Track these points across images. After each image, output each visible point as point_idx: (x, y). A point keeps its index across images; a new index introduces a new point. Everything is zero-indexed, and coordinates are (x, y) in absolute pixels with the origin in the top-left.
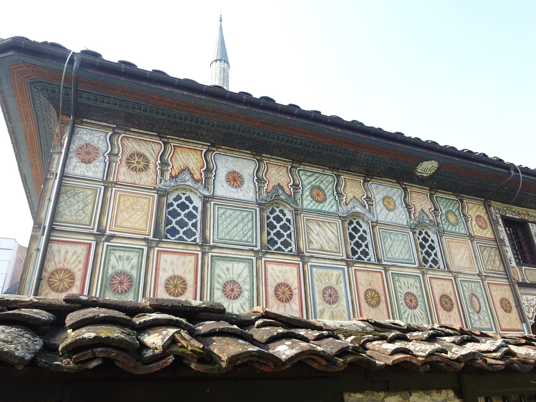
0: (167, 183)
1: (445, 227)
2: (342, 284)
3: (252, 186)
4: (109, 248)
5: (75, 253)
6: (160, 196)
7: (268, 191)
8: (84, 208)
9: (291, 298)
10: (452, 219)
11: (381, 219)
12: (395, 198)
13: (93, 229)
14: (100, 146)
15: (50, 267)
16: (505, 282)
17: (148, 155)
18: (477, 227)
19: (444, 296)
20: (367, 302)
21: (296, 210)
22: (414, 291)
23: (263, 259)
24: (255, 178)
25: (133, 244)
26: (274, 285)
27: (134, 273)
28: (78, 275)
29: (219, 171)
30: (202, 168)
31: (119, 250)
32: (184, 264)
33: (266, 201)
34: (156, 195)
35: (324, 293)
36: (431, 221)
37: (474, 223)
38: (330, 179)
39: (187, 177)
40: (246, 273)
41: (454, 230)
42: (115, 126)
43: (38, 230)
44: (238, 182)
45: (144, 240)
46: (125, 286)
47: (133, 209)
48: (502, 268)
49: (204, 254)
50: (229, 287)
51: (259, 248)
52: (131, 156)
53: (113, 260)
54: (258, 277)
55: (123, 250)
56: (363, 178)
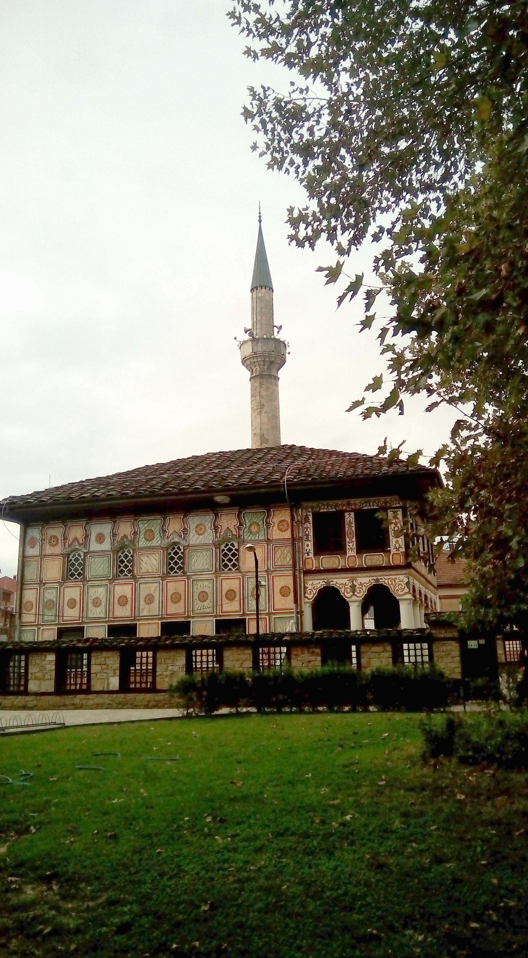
1: (246, 537)
3: (109, 540)
10: (254, 529)
11: (192, 543)
12: (206, 524)
15: (24, 601)
17: (58, 536)
18: (278, 531)
27: (55, 599)
35: (146, 598)
36: (233, 535)
37: (275, 528)
38: (159, 521)
39: (76, 543)
40: (104, 592)
45: (58, 582)
48: (291, 563)
54: (110, 593)
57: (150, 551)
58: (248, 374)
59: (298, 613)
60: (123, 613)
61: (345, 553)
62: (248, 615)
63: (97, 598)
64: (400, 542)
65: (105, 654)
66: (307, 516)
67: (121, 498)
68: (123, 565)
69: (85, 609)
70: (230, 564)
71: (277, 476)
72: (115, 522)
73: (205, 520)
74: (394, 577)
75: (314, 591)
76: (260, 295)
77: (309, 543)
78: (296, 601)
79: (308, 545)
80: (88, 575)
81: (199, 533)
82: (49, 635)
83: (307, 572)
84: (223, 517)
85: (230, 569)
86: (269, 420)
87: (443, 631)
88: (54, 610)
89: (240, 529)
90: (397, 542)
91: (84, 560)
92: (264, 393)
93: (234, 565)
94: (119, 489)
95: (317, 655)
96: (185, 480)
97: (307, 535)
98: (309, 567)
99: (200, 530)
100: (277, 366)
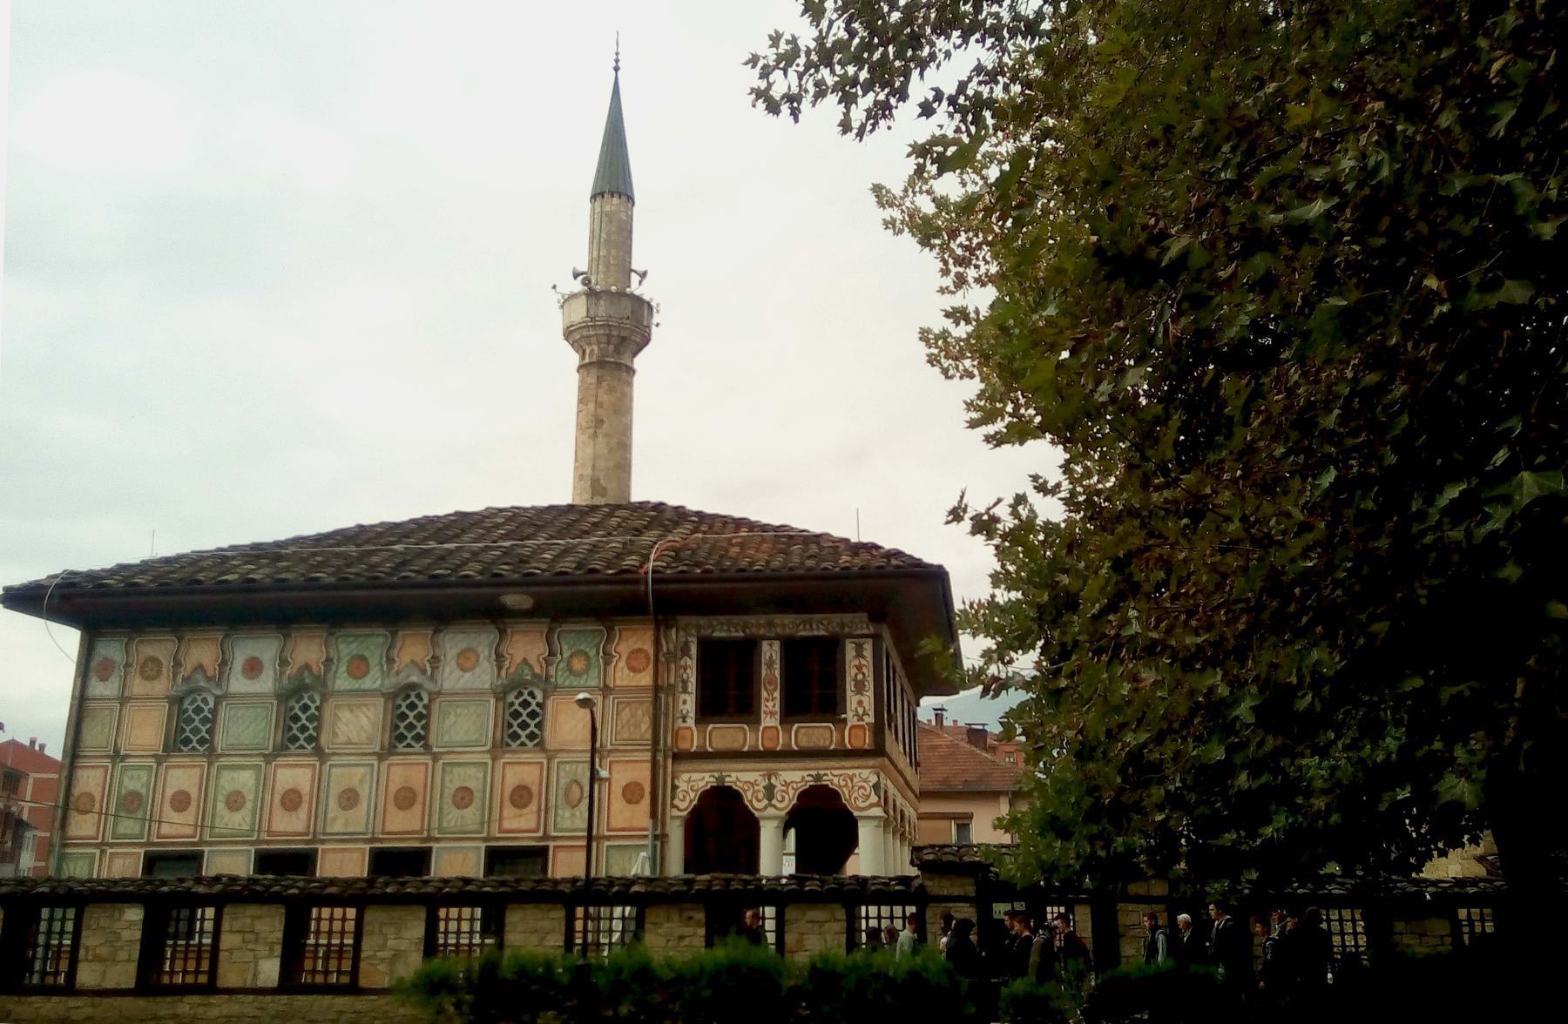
0: (181, 687)
1: (560, 681)
2: (367, 785)
10: (578, 665)
11: (446, 686)
12: (480, 649)
15: (76, 792)
16: (647, 756)
18: (626, 671)
22: (472, 784)
27: (143, 791)
28: (98, 798)
35: (340, 796)
36: (535, 675)
37: (622, 664)
38: (381, 640)
39: (199, 676)
48: (649, 735)
53: (126, 779)
58: (574, 359)
59: (656, 837)
60: (288, 828)
61: (759, 722)
63: (238, 793)
64: (866, 704)
65: (253, 910)
66: (687, 643)
67: (305, 589)
68: (298, 724)
70: (523, 734)
71: (631, 561)
73: (481, 641)
74: (850, 772)
75: (692, 795)
76: (608, 208)
77: (687, 697)
78: (653, 815)
79: (685, 702)
80: (220, 741)
81: (465, 669)
82: (125, 866)
83: (679, 757)
84: (516, 638)
85: (523, 744)
86: (611, 450)
87: (945, 883)
89: (548, 663)
90: (860, 703)
91: (214, 712)
92: (604, 397)
93: (532, 736)
94: (301, 568)
95: (698, 925)
96: (442, 558)
97: (685, 683)
98: (684, 746)
99: (466, 661)
100: (633, 347)
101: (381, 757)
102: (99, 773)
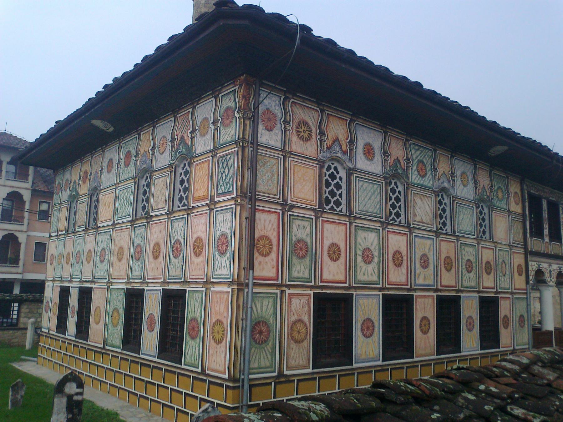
1: (495, 202)
2: (432, 253)
3: (380, 159)
4: (292, 217)
5: (270, 221)
6: (321, 167)
7: (391, 165)
8: (271, 178)
9: (402, 263)
12: (468, 174)
13: (279, 199)
14: (277, 111)
16: (522, 251)
17: (311, 124)
19: (488, 263)
20: (445, 267)
21: (408, 184)
22: (472, 258)
23: (386, 229)
24: (382, 151)
25: (306, 214)
26: (392, 252)
27: (308, 240)
29: (358, 143)
30: (347, 139)
31: (298, 219)
32: (338, 233)
33: (389, 175)
34: (318, 166)
36: (488, 196)
37: (512, 198)
38: (430, 153)
40: (376, 242)
41: (500, 205)
42: (285, 90)
43: (244, 199)
44: (372, 155)
45: (313, 210)
46: (304, 252)
47: (304, 180)
48: (522, 240)
49: (351, 224)
50: (366, 254)
51: (383, 219)
52: (299, 124)
53: (295, 229)
55: (300, 220)
56: (450, 153)
57: (423, 193)
62: (500, 293)
69: (353, 264)
72: (386, 133)
88: (307, 260)
101: (437, 235)
102: (273, 218)
